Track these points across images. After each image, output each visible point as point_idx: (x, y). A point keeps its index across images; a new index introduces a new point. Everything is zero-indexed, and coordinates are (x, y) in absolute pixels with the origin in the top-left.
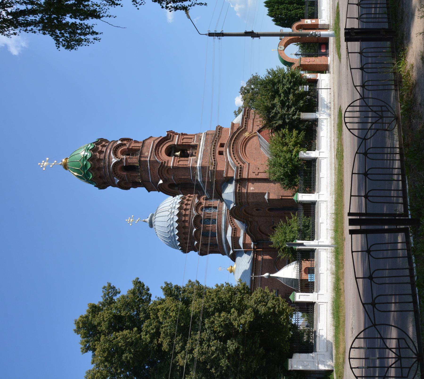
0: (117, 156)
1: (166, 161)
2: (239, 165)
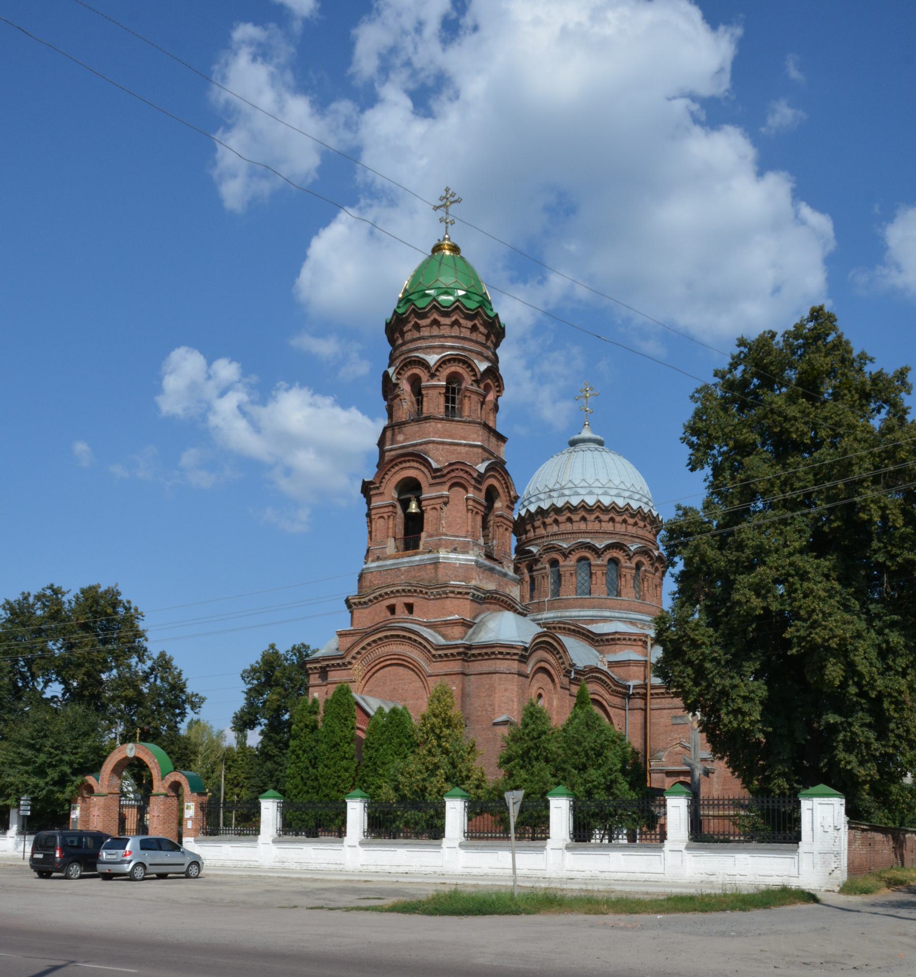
0: (404, 370)
1: (381, 490)
2: (348, 659)
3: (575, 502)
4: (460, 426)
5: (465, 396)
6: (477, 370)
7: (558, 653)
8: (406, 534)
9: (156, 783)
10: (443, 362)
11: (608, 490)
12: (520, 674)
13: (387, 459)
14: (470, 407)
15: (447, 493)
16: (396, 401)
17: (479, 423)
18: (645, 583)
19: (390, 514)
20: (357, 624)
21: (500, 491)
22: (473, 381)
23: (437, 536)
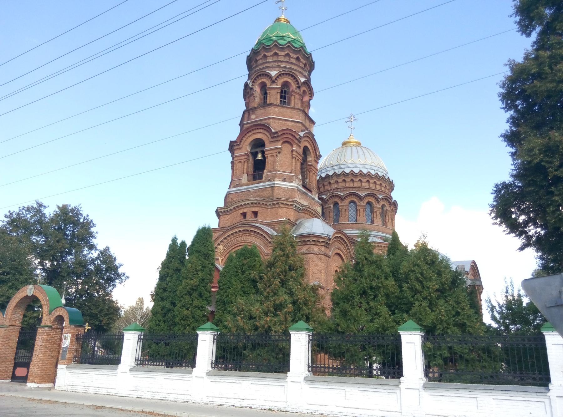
1: (241, 146)
3: (347, 171)
4: (289, 111)
5: (292, 95)
6: (299, 81)
7: (347, 245)
8: (254, 172)
9: (45, 318)
10: (279, 76)
11: (366, 166)
12: (325, 255)
13: (244, 128)
14: (294, 102)
15: (280, 147)
16: (251, 98)
17: (300, 110)
18: (387, 217)
19: (245, 160)
20: (222, 225)
21: (311, 151)
22: (297, 87)
23: (274, 171)
